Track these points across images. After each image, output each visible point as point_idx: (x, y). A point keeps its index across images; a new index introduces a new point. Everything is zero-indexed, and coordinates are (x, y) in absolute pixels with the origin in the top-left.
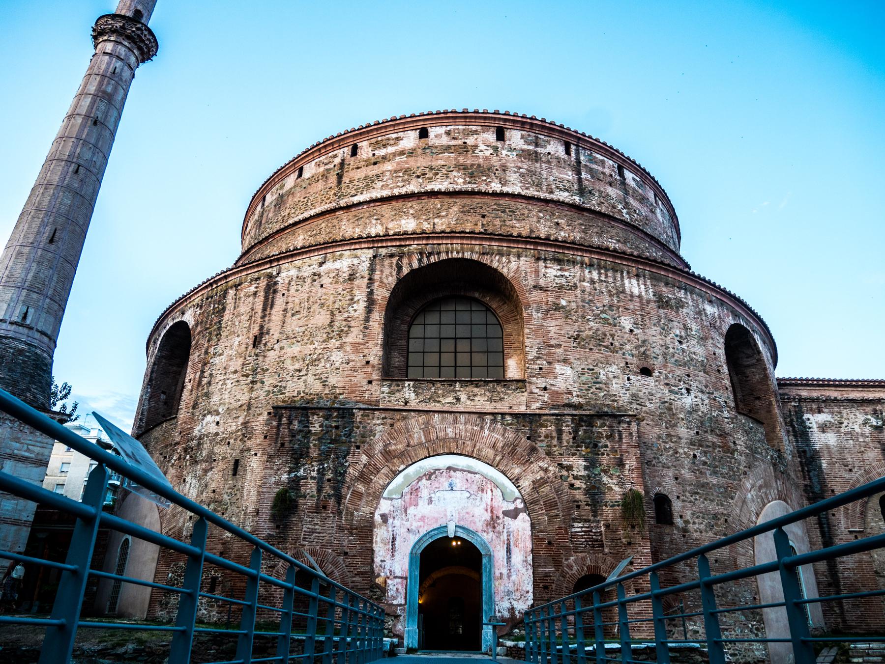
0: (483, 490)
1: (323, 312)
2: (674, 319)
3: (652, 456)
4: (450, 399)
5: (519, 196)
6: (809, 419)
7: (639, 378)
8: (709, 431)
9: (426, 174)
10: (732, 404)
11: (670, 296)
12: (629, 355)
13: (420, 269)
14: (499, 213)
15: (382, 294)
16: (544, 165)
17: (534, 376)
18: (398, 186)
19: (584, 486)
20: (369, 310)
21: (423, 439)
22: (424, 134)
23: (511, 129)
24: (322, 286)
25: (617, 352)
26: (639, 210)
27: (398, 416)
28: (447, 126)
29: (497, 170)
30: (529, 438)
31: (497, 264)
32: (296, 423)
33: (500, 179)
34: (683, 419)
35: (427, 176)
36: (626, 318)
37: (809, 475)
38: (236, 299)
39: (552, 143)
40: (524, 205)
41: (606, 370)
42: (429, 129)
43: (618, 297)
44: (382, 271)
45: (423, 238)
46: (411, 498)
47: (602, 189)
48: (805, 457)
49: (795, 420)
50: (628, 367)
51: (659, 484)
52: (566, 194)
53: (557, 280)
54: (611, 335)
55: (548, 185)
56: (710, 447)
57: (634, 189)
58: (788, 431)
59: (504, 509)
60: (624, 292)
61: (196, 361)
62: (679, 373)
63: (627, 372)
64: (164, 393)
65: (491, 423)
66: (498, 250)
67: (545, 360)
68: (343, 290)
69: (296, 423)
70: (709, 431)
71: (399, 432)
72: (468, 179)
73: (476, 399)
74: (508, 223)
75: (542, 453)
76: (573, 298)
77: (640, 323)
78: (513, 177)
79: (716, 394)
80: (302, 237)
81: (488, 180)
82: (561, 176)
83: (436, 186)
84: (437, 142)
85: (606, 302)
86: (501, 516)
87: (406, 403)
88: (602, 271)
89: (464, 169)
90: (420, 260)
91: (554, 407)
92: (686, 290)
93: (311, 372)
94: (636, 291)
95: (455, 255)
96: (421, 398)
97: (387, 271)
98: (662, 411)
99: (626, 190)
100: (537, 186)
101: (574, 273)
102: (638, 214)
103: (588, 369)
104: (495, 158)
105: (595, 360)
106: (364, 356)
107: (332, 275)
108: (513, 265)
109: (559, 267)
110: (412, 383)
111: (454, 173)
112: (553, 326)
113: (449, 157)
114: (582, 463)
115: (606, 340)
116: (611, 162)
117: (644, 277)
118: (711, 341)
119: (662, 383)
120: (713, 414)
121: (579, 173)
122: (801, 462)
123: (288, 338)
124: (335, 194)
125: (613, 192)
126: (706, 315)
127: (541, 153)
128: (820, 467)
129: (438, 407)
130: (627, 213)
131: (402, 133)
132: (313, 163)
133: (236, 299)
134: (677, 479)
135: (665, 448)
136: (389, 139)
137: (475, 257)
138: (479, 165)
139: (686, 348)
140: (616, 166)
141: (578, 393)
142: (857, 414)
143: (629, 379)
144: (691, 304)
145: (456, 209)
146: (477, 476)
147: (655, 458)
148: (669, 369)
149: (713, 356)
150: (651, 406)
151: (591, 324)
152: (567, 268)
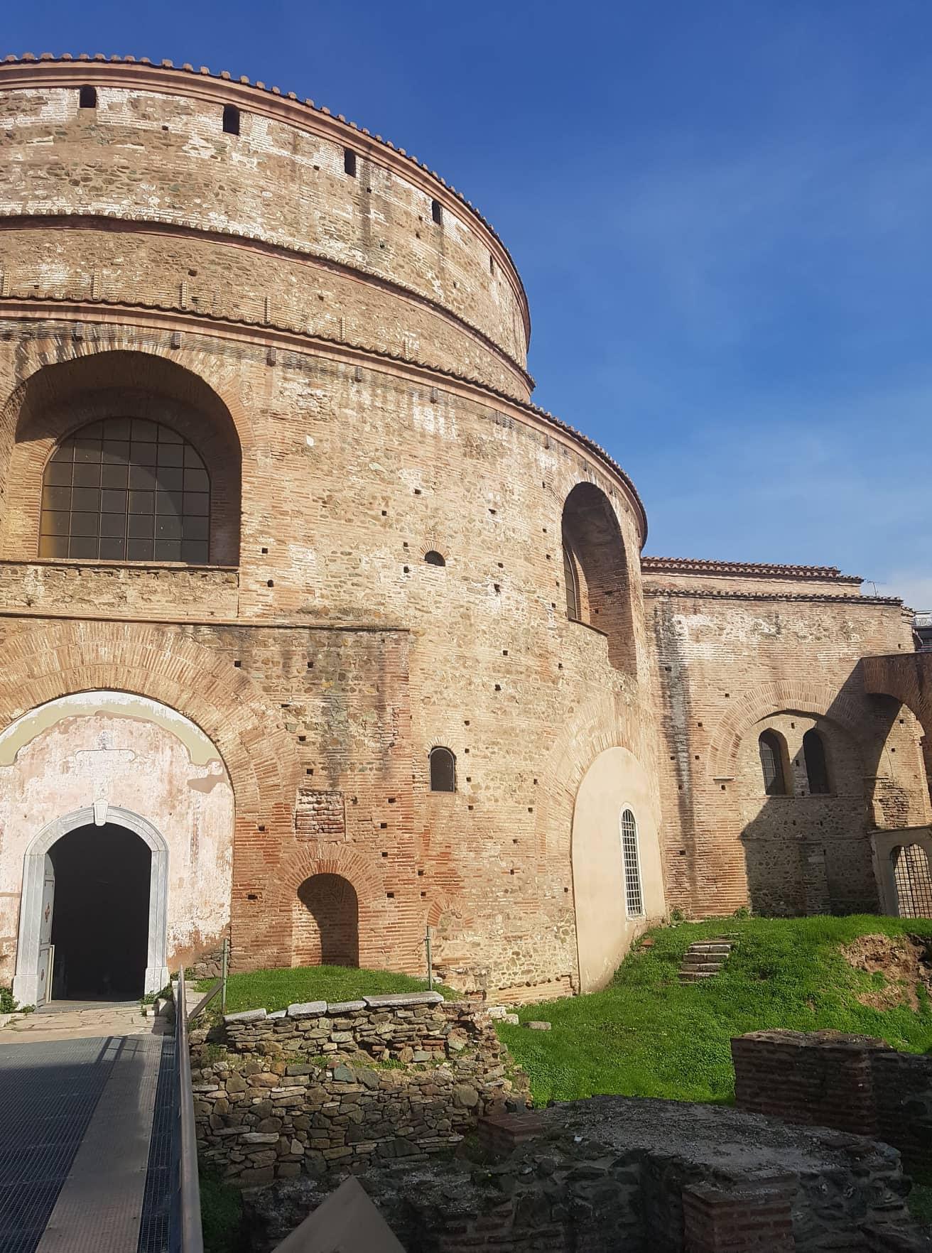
0: (157, 748)
2: (487, 475)
3: (433, 689)
4: (107, 598)
5: (255, 242)
6: (680, 622)
8: (523, 650)
9: (90, 180)
10: (564, 608)
11: (484, 437)
13: (61, 365)
14: (219, 269)
16: (305, 188)
18: (37, 197)
19: (320, 739)
22: (88, 99)
25: (391, 526)
28: (132, 89)
30: (238, 664)
33: (227, 206)
35: (91, 184)
40: (265, 259)
41: (371, 555)
45: (67, 309)
46: (31, 764)
47: (402, 242)
49: (661, 623)
50: (408, 551)
51: (440, 732)
52: (340, 245)
54: (383, 498)
55: (310, 226)
59: (190, 778)
60: (410, 428)
62: (486, 560)
63: (405, 559)
66: (203, 343)
67: (273, 537)
72: (167, 199)
74: (236, 289)
75: (257, 688)
78: (248, 204)
79: (540, 593)
81: (204, 206)
83: (109, 207)
84: (114, 120)
85: (380, 441)
86: (186, 789)
87: (29, 605)
88: (379, 392)
90: (60, 349)
91: (284, 612)
94: (431, 428)
95: (125, 346)
98: (454, 620)
100: (291, 225)
101: (332, 390)
102: (459, 290)
103: (342, 553)
108: (229, 371)
110: (40, 568)
111: (144, 186)
112: (288, 479)
113: (135, 151)
115: (375, 506)
116: (422, 195)
117: (446, 404)
118: (541, 510)
120: (532, 624)
121: (365, 210)
125: (422, 249)
127: (302, 166)
128: (686, 692)
129: (88, 611)
130: (441, 286)
134: (467, 723)
137: (162, 352)
138: (190, 175)
139: (501, 521)
140: (430, 203)
142: (745, 617)
143: (406, 570)
144: (516, 451)
145: (143, 253)
146: (148, 725)
149: (543, 534)
152: (320, 382)
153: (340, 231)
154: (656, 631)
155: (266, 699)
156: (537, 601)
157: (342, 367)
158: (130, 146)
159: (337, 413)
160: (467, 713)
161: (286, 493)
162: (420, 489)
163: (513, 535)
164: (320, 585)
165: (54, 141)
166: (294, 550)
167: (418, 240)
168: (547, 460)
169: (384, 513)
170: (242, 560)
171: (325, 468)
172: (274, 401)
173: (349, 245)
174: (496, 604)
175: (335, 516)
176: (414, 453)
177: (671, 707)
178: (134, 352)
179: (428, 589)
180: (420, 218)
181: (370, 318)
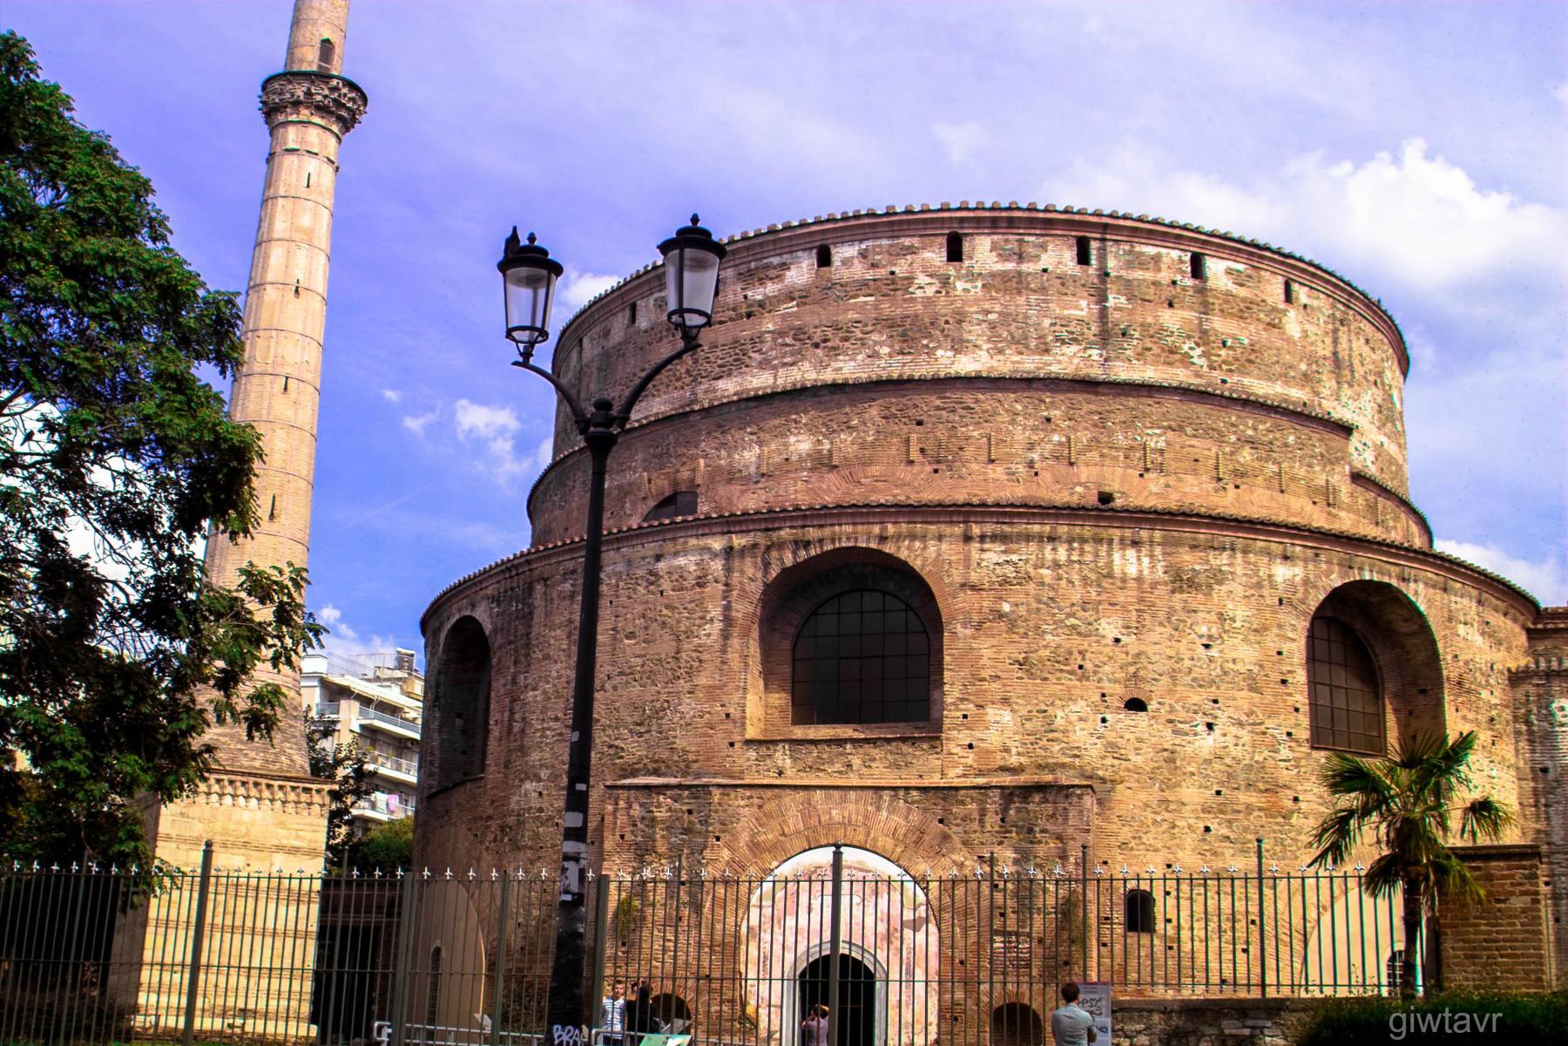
1: (666, 637)
4: (838, 767)
6: (1562, 709)
7: (1122, 716)
8: (1243, 788)
9: (826, 341)
11: (1197, 567)
12: (1109, 680)
13: (797, 566)
14: (944, 413)
15: (744, 609)
16: (1033, 298)
17: (954, 729)
18: (785, 364)
20: (725, 635)
21: (801, 826)
22: (824, 259)
23: (972, 234)
24: (662, 592)
25: (1088, 679)
26: (1235, 338)
27: (769, 793)
28: (861, 241)
29: (947, 322)
30: (941, 821)
31: (906, 553)
32: (636, 806)
33: (953, 340)
34: (1193, 774)
35: (829, 344)
36: (1110, 620)
37: (1546, 813)
38: (548, 600)
39: (1050, 247)
42: (832, 247)
43: (1099, 585)
44: (742, 572)
45: (797, 518)
47: (1150, 320)
48: (1545, 781)
49: (1535, 710)
53: (999, 571)
54: (1080, 652)
55: (1040, 338)
56: (1239, 812)
57: (1228, 294)
58: (1518, 733)
60: (1110, 575)
61: (502, 692)
62: (1196, 699)
64: (459, 715)
65: (892, 801)
67: (973, 702)
68: (691, 602)
69: (636, 806)
70: (1243, 788)
71: (769, 816)
73: (874, 765)
76: (1021, 598)
77: (1135, 625)
78: (975, 332)
79: (1269, 723)
80: (640, 457)
82: (1066, 312)
85: (1077, 595)
87: (780, 773)
88: (1076, 545)
89: (890, 327)
92: (1233, 549)
93: (655, 728)
94: (1132, 571)
96: (801, 765)
97: (750, 571)
98: (1155, 765)
99: (1205, 304)
100: (1018, 343)
102: (1231, 348)
104: (942, 299)
105: (1051, 695)
106: (722, 706)
107: (676, 576)
108: (932, 550)
109: (1003, 548)
112: (986, 649)
113: (866, 303)
114: (1010, 854)
115: (1072, 662)
116: (1175, 254)
118: (1275, 630)
119: (1163, 720)
121: (1102, 298)
122: (1535, 789)
123: (621, 673)
124: (688, 372)
126: (1273, 586)
127: (1029, 274)
131: (788, 256)
132: (651, 301)
133: (548, 600)
135: (1155, 822)
136: (768, 267)
137: (873, 545)
138: (916, 316)
139: (1217, 655)
141: (1020, 750)
143: (1104, 720)
147: (1134, 838)
148: (1177, 696)
150: (1138, 760)
151: (1048, 637)
153: (1073, 333)
154: (1528, 723)
155: (965, 851)
156: (1264, 733)
157: (1036, 528)
158: (862, 299)
159: (1032, 575)
160: (1170, 856)
161: (985, 661)
162: (1119, 636)
163: (1231, 666)
164: (1017, 744)
165: (798, 306)
166: (992, 713)
167: (1169, 312)
168: (1282, 572)
169: (1081, 667)
170: (945, 727)
171: (1022, 630)
172: (973, 574)
173: (1084, 345)
174: (1206, 743)
175: (1032, 676)
176: (1113, 600)
177: (1548, 819)
178: (851, 548)
179: (1127, 737)
180: (1174, 283)
181: (1104, 427)
